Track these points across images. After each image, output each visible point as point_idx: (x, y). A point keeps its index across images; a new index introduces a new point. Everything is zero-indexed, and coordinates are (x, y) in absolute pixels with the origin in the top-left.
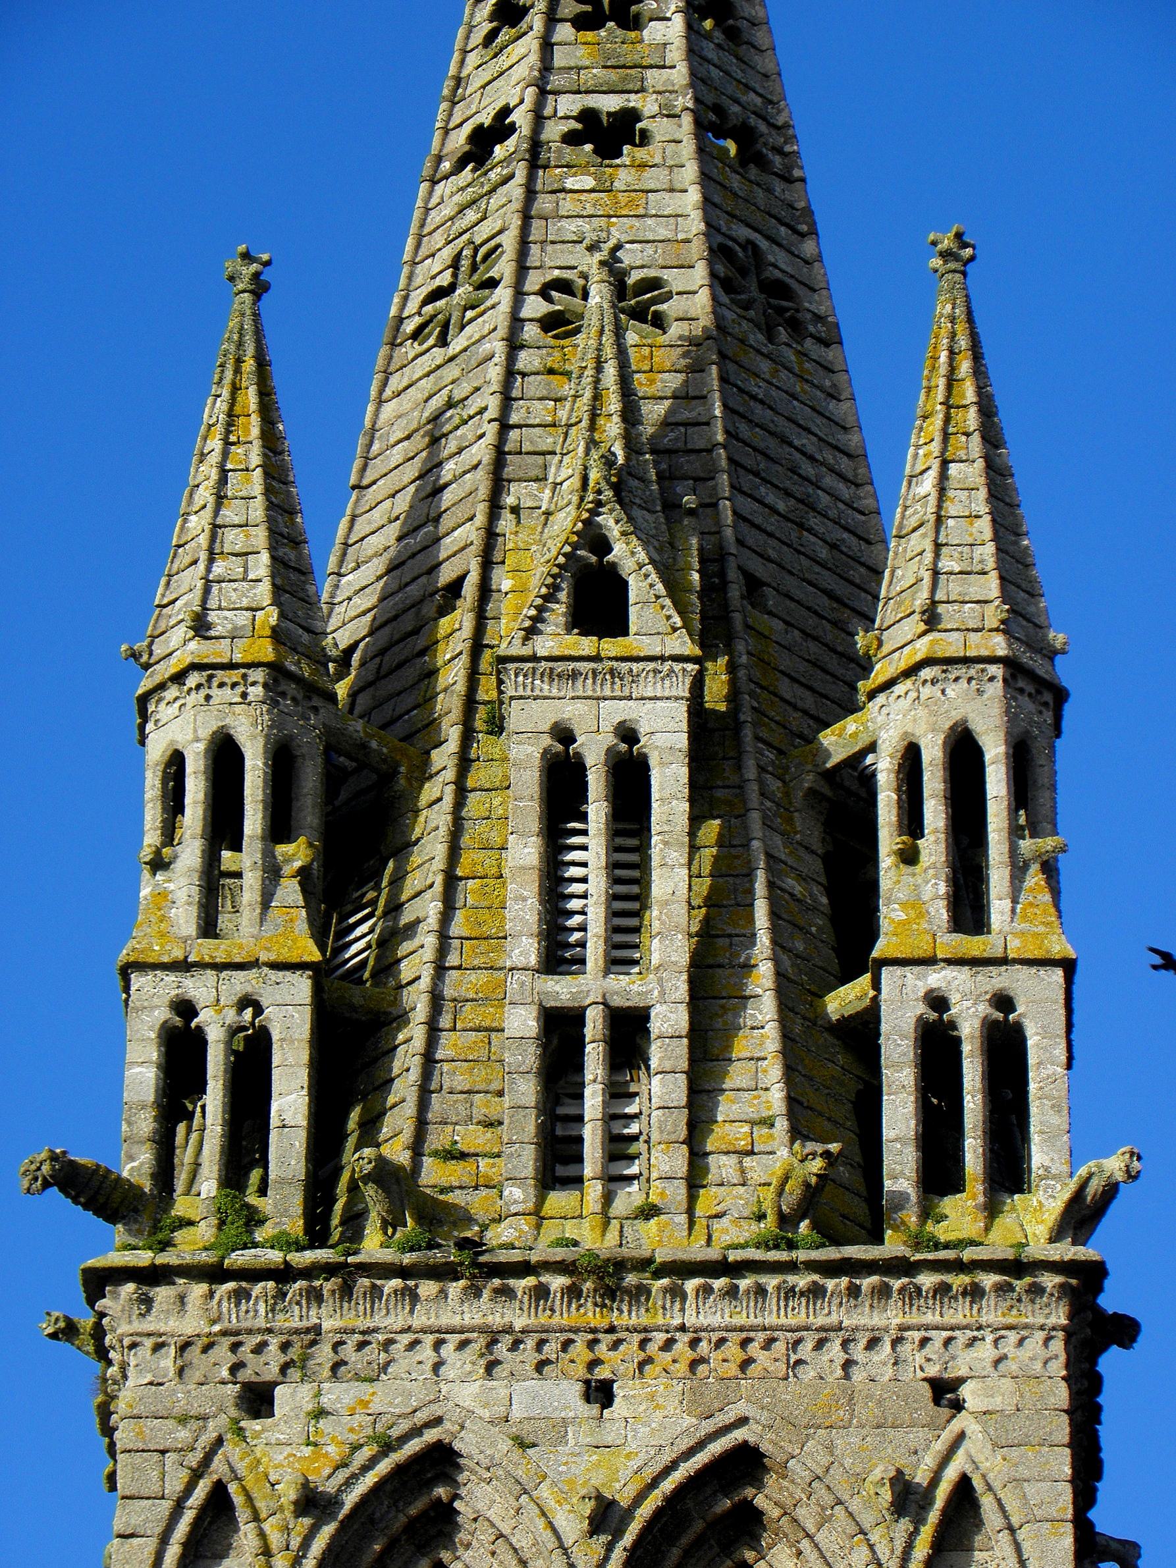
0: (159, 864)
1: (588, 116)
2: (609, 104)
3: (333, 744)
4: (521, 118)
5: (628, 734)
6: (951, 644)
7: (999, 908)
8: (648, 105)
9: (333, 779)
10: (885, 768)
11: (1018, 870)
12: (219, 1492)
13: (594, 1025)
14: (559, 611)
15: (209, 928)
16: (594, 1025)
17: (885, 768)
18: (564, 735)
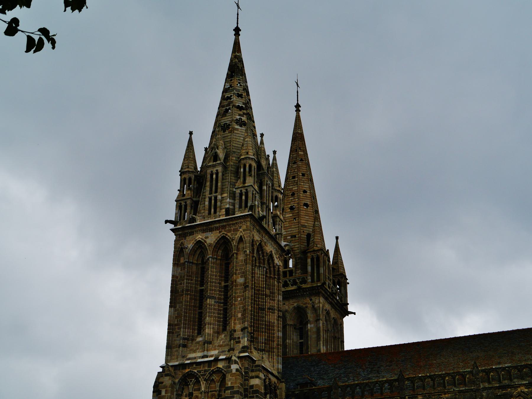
5: (217, 170)
13: (213, 198)
14: (212, 160)
16: (213, 198)
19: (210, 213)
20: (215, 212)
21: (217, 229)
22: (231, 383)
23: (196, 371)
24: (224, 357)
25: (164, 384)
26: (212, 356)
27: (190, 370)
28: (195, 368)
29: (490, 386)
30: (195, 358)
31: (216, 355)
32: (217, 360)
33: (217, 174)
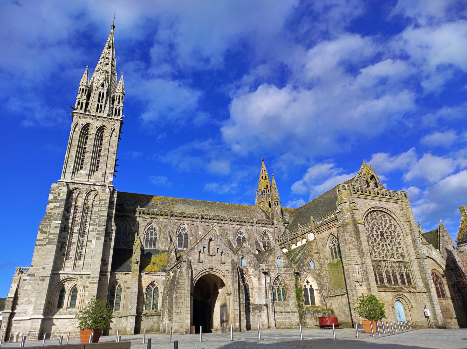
0: (79, 94)
1: (106, 63)
2: (107, 63)
3: (89, 90)
4: (103, 62)
5: (103, 92)
6: (120, 91)
7: (120, 104)
8: (109, 63)
9: (88, 91)
10: (116, 96)
11: (121, 102)
12: (78, 123)
15: (81, 97)
17: (116, 96)
18: (100, 92)
19: (97, 111)
20: (101, 112)
21: (100, 120)
22: (105, 198)
23: (81, 188)
24: (99, 184)
25: (62, 190)
26: (92, 182)
27: (77, 186)
28: (81, 186)
29: (205, 221)
30: (81, 181)
31: (94, 182)
32: (95, 185)
33: (103, 94)
